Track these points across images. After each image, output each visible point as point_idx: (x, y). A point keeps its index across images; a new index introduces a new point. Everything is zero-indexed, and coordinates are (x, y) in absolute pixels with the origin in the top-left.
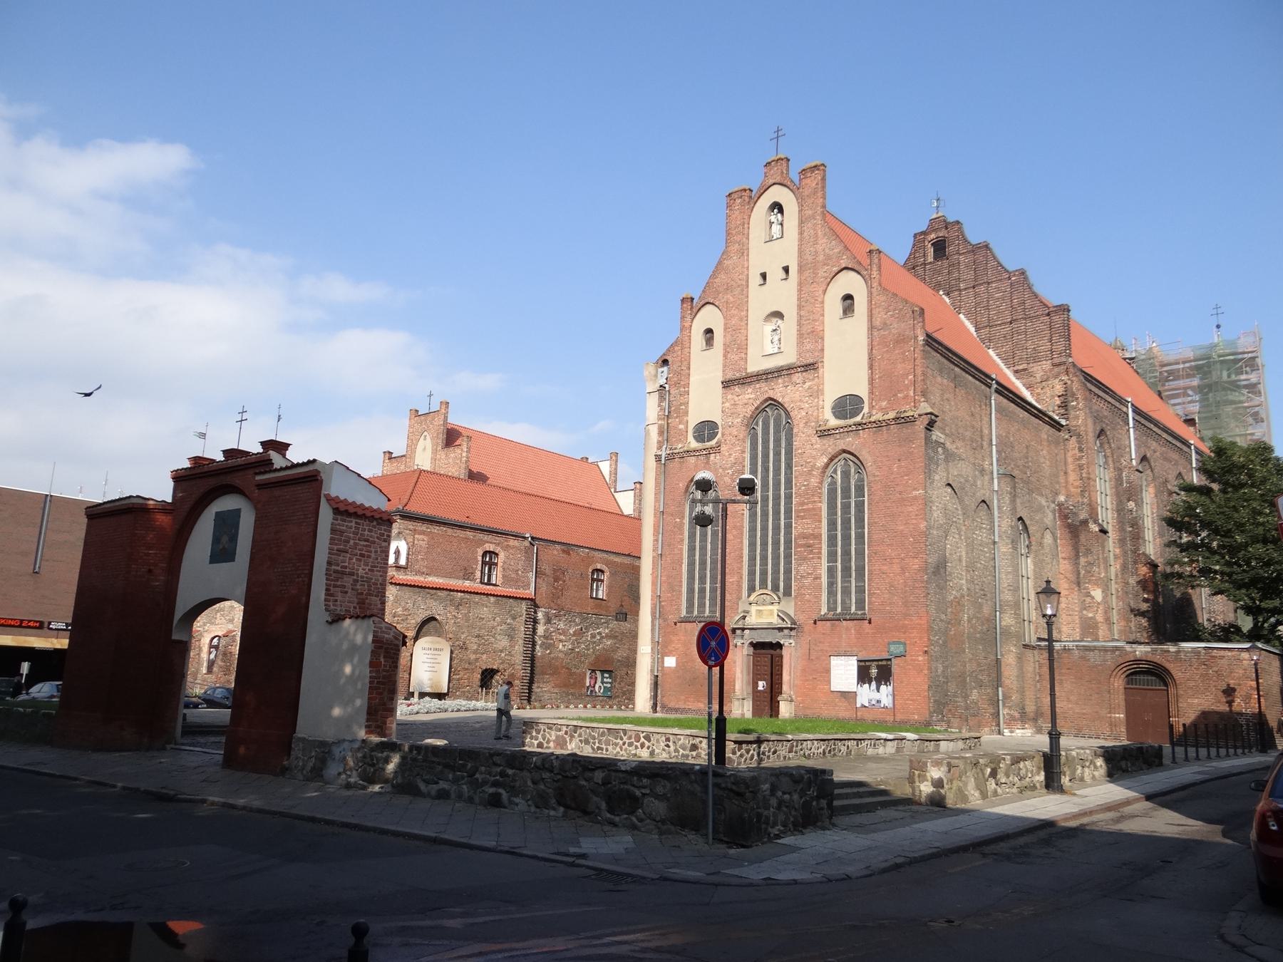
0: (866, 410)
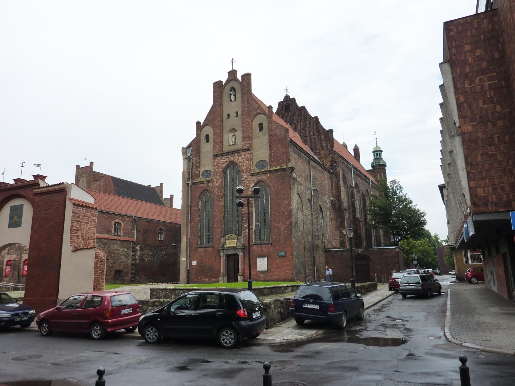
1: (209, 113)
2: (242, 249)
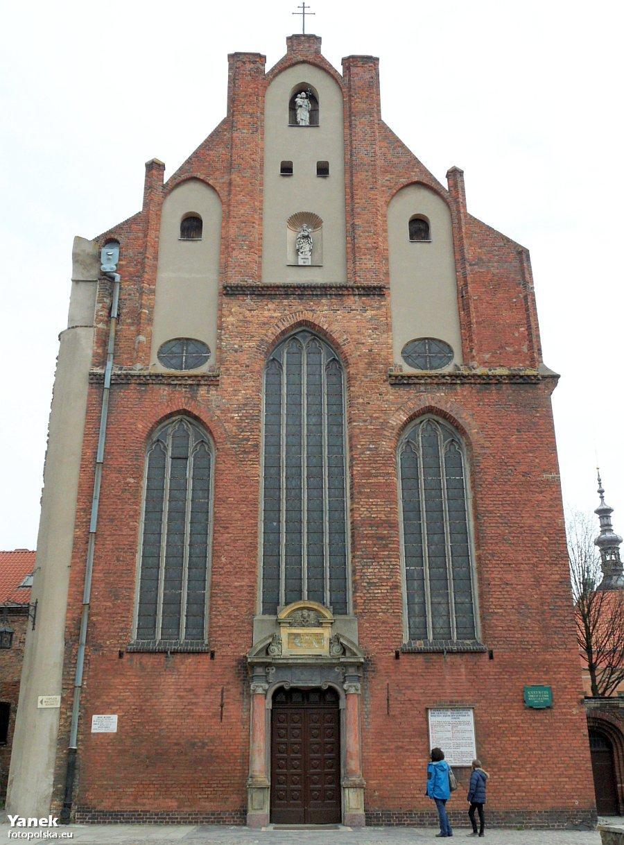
0: (457, 359)
1: (206, 141)
2: (359, 666)
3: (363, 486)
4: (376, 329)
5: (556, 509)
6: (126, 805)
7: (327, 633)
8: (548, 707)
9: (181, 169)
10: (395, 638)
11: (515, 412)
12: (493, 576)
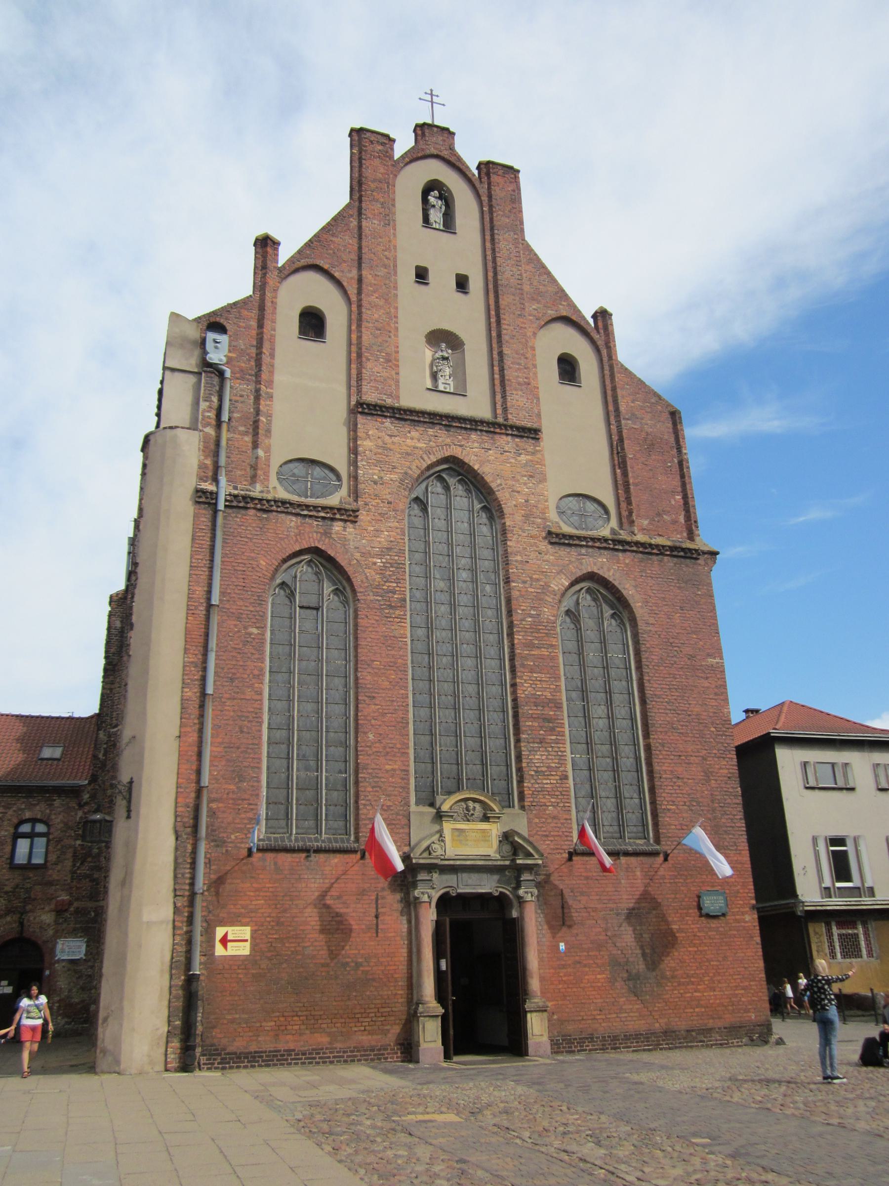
1: (329, 224)
3: (526, 658)
4: (531, 476)
5: (722, 697)
6: (266, 1043)
7: (495, 830)
8: (724, 915)
9: (300, 252)
10: (567, 836)
11: (678, 587)
12: (664, 768)
